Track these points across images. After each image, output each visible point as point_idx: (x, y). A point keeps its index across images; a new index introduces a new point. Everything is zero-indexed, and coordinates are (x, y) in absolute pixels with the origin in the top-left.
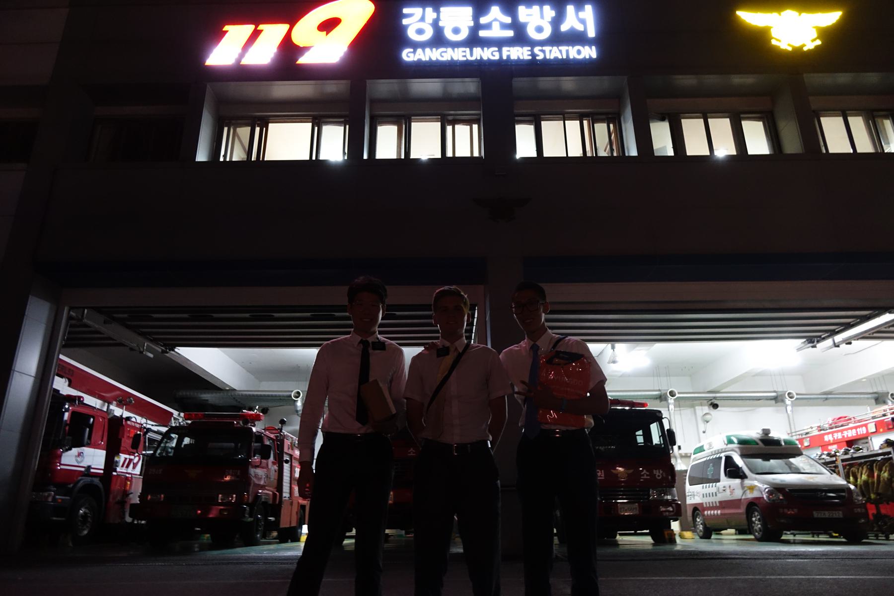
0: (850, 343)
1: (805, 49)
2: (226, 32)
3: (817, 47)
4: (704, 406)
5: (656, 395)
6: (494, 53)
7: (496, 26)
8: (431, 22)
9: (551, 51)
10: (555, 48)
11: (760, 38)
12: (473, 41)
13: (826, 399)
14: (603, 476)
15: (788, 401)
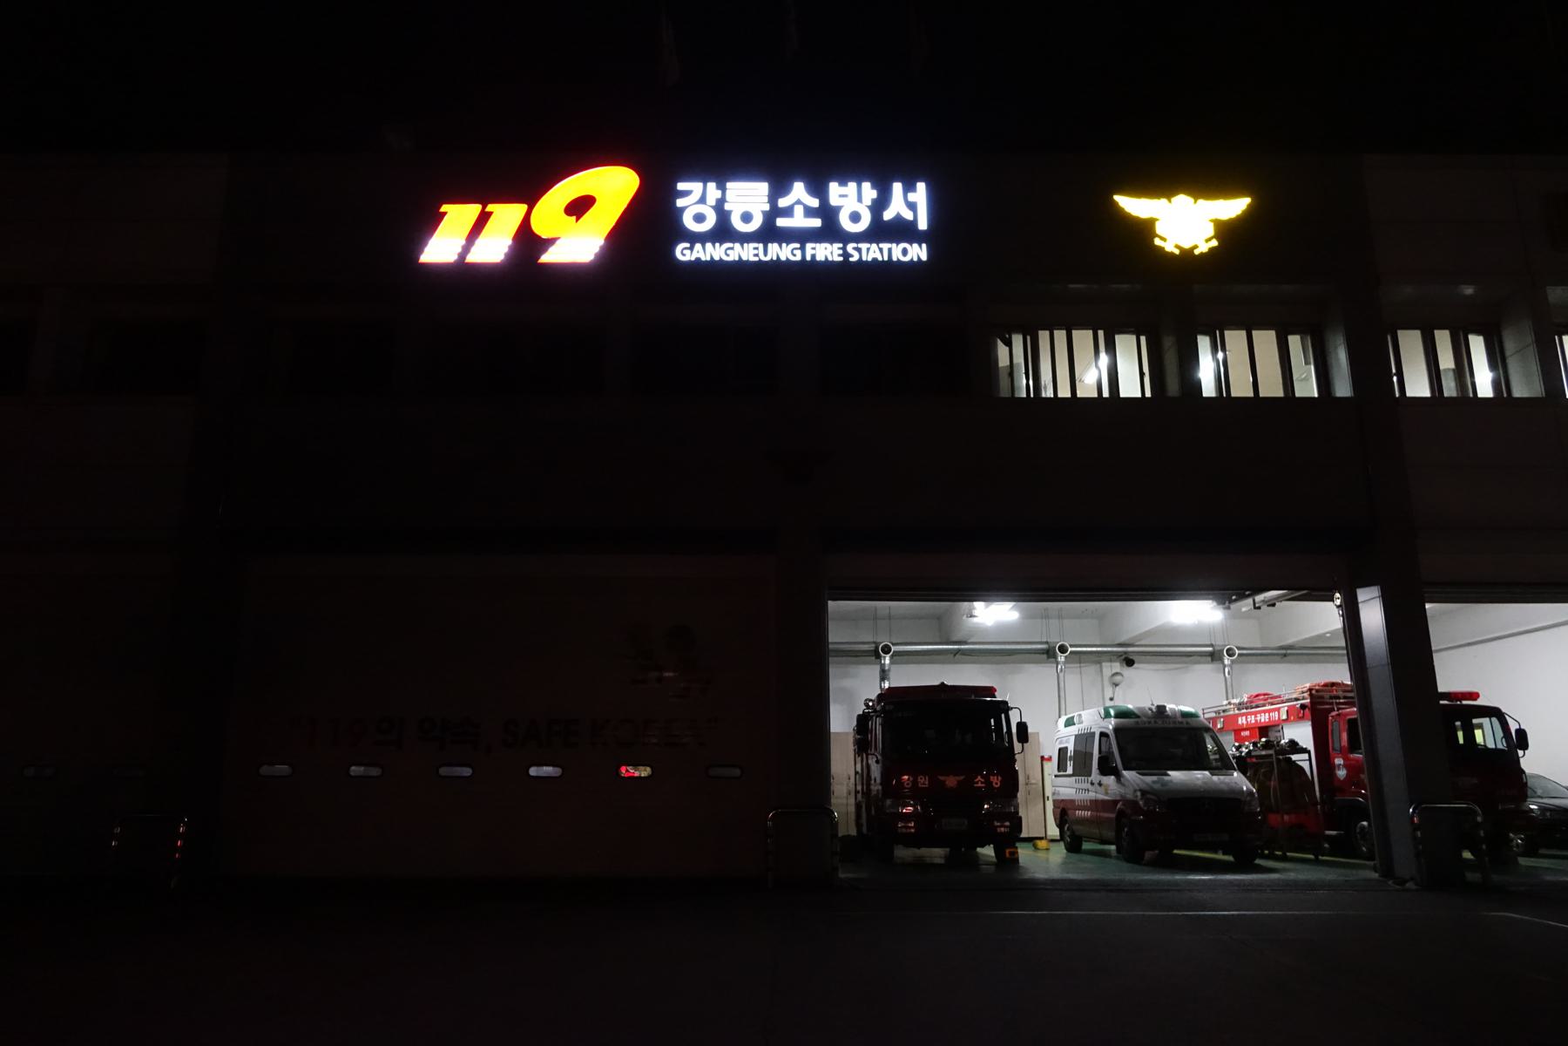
0: (1274, 605)
1: (1197, 252)
2: (445, 214)
3: (1212, 250)
4: (1115, 661)
5: (1043, 649)
6: (795, 252)
7: (799, 210)
8: (714, 203)
9: (868, 249)
10: (874, 246)
11: (1143, 230)
12: (770, 233)
13: (1285, 655)
14: (927, 783)
15: (1227, 661)
